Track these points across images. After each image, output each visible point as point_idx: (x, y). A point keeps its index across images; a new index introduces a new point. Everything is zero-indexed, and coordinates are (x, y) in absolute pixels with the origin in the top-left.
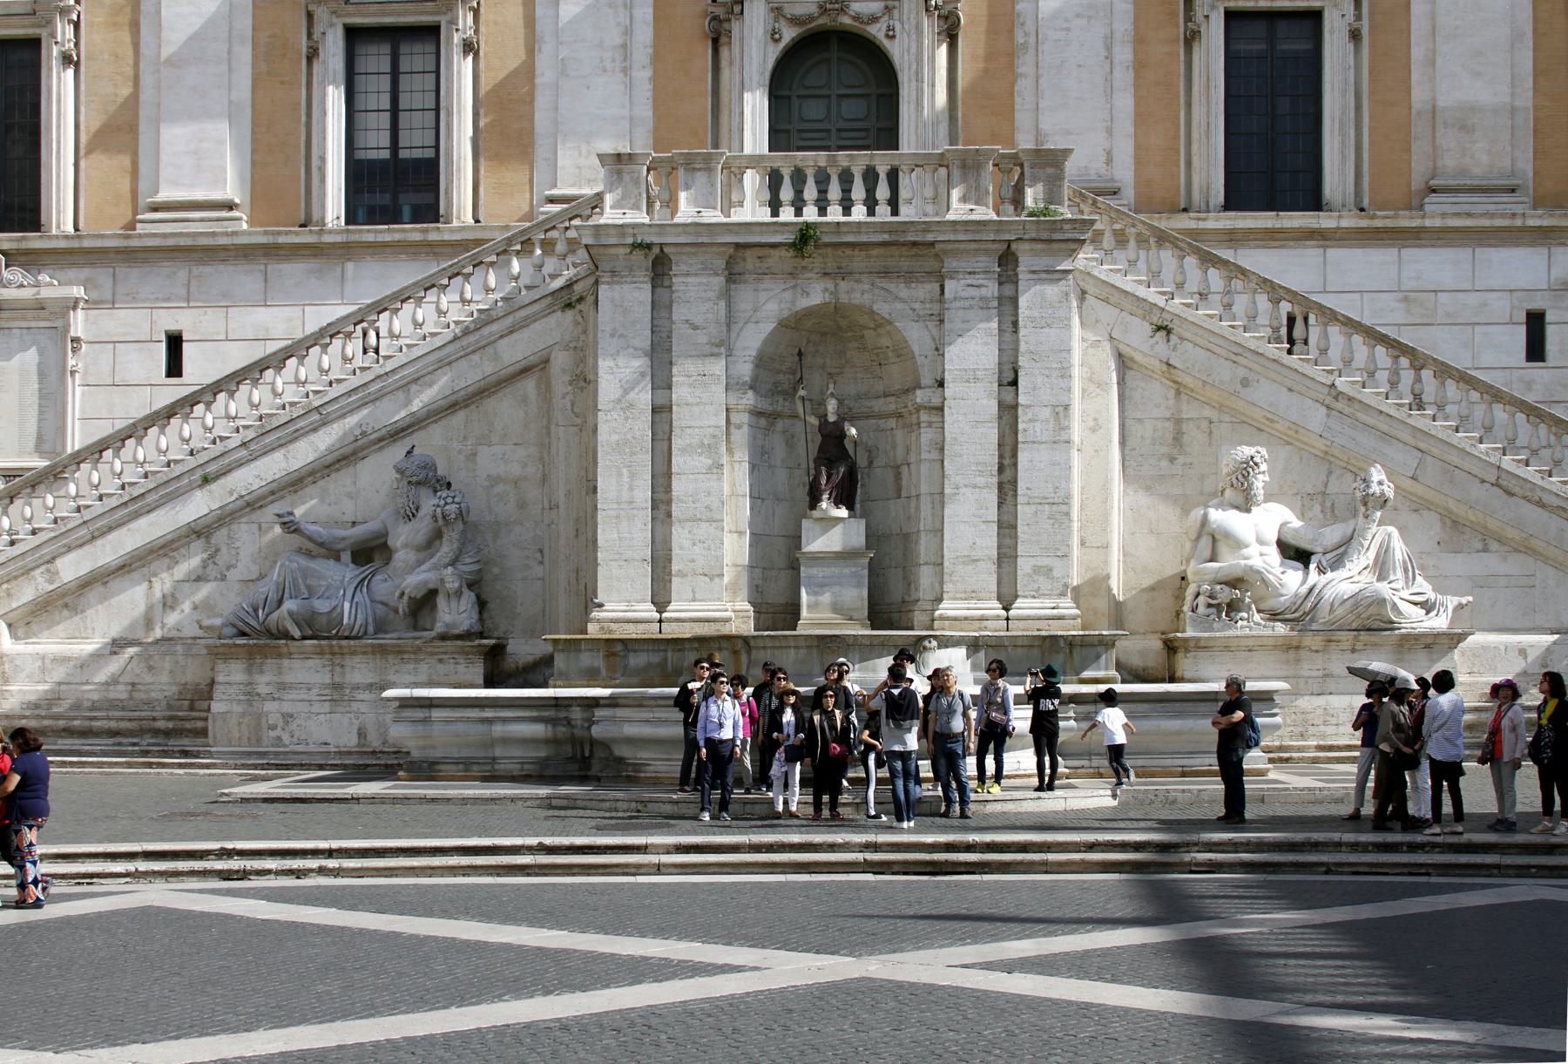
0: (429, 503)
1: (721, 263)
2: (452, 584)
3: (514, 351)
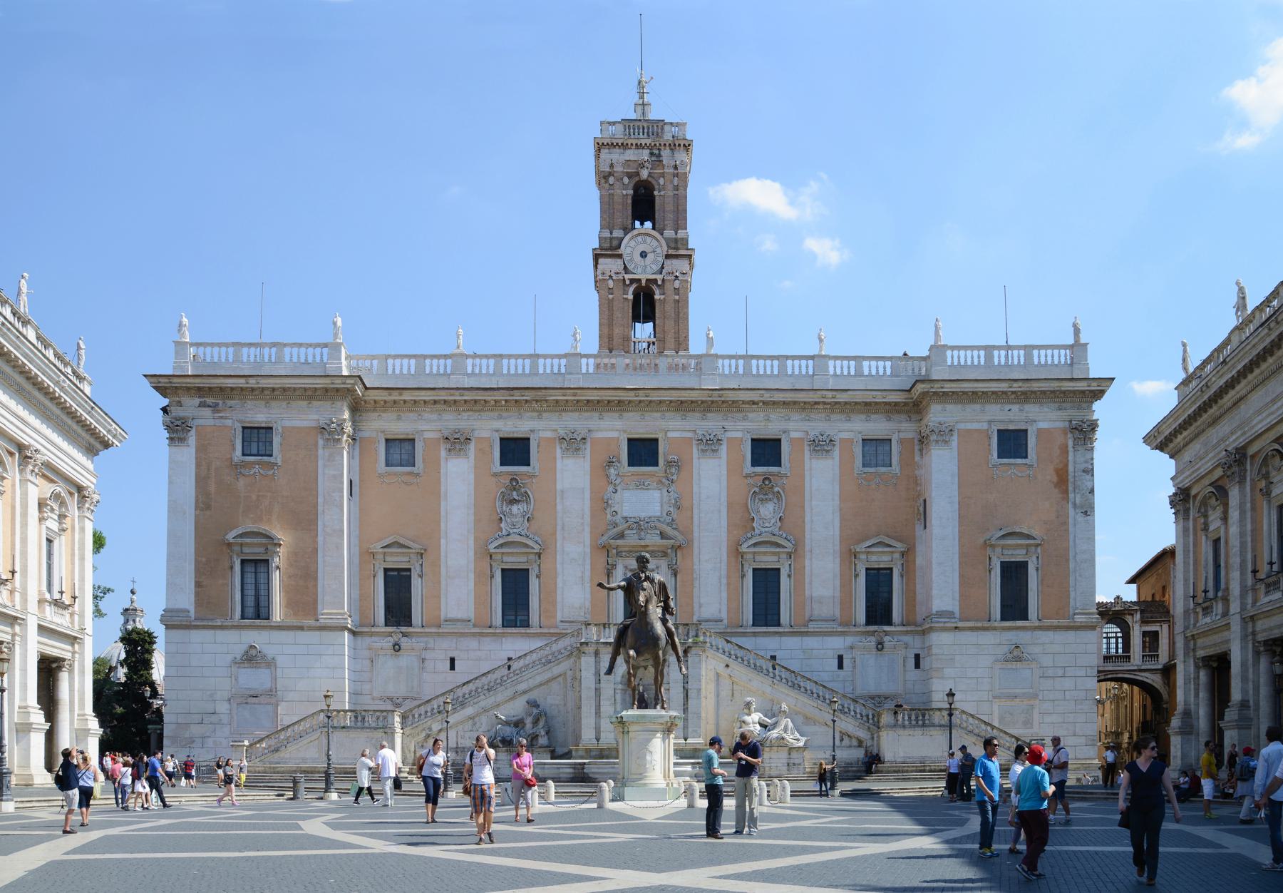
2: (543, 733)
3: (557, 670)
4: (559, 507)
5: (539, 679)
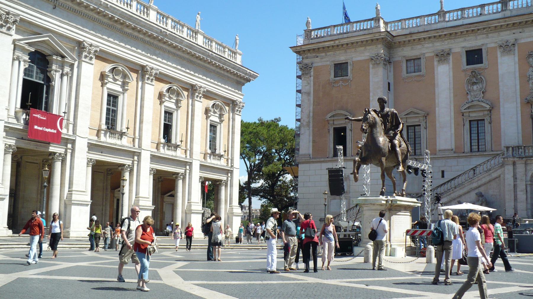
0: (481, 199)
1: (524, 162)
3: (494, 175)
4: (500, 84)
5: (484, 181)
